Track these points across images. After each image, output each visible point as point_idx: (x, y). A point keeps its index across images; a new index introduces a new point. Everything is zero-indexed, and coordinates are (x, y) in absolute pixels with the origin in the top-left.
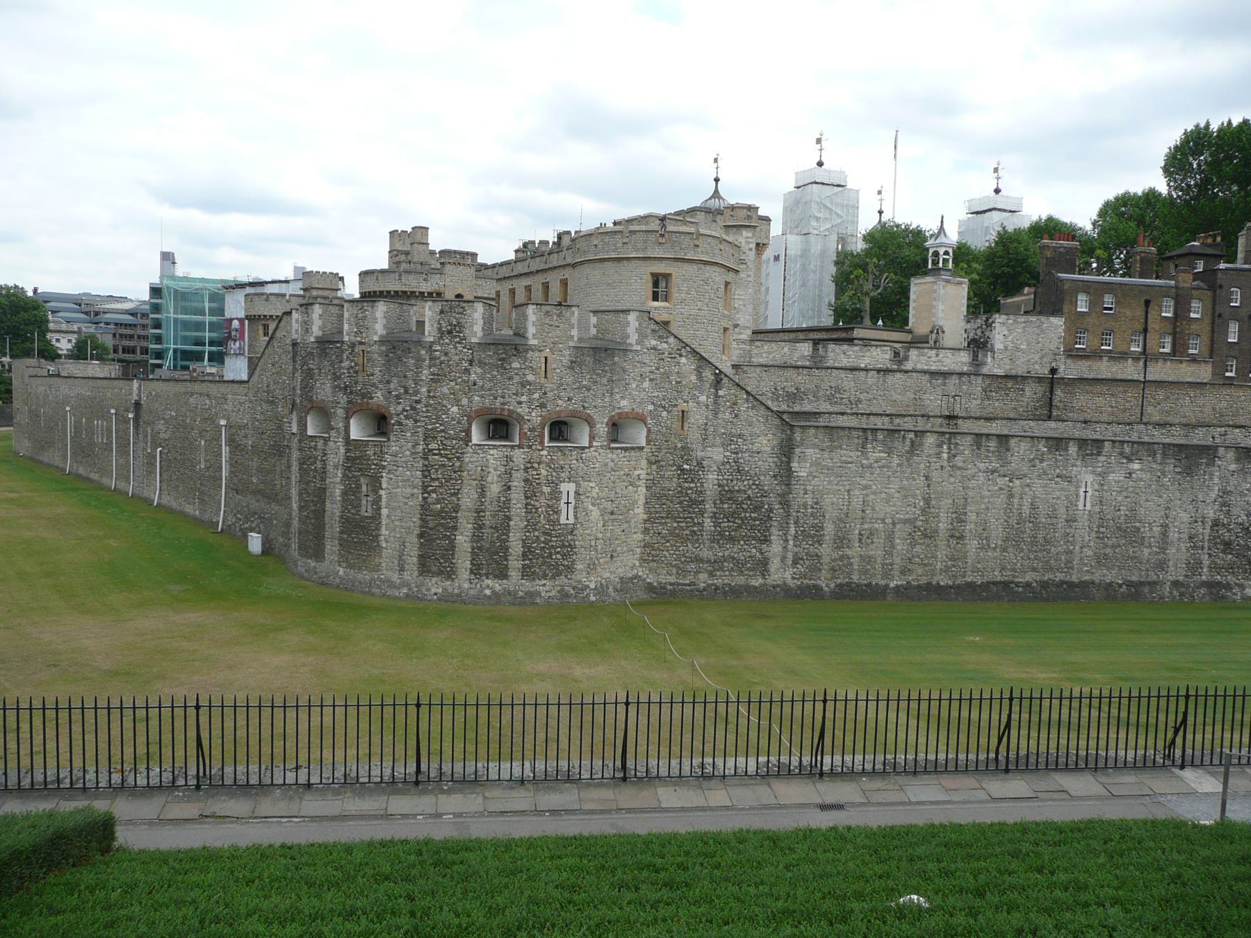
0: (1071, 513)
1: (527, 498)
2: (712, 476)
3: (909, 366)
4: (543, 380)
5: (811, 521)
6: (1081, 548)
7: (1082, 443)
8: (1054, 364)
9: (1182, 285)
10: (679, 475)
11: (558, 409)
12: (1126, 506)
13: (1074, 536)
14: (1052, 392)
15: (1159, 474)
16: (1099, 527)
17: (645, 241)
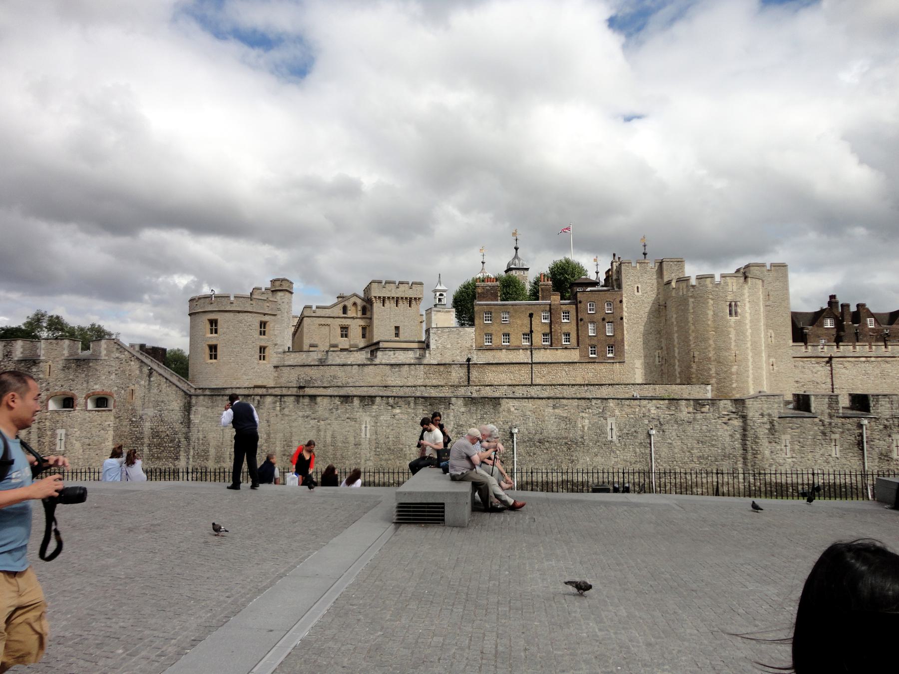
0: (357, 440)
1: (39, 437)
2: (147, 426)
3: (377, 361)
4: (47, 377)
5: (202, 447)
6: (365, 461)
7: (362, 398)
8: (469, 356)
9: (553, 303)
10: (130, 424)
11: (56, 391)
12: (393, 435)
13: (360, 454)
14: (469, 372)
15: (413, 415)
16: (376, 448)
17: (204, 303)
